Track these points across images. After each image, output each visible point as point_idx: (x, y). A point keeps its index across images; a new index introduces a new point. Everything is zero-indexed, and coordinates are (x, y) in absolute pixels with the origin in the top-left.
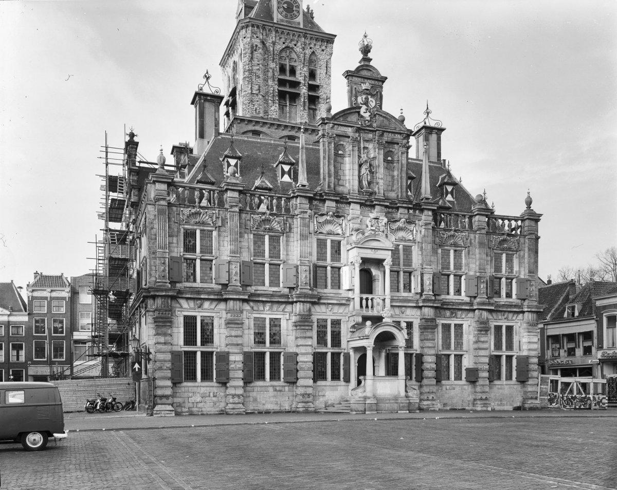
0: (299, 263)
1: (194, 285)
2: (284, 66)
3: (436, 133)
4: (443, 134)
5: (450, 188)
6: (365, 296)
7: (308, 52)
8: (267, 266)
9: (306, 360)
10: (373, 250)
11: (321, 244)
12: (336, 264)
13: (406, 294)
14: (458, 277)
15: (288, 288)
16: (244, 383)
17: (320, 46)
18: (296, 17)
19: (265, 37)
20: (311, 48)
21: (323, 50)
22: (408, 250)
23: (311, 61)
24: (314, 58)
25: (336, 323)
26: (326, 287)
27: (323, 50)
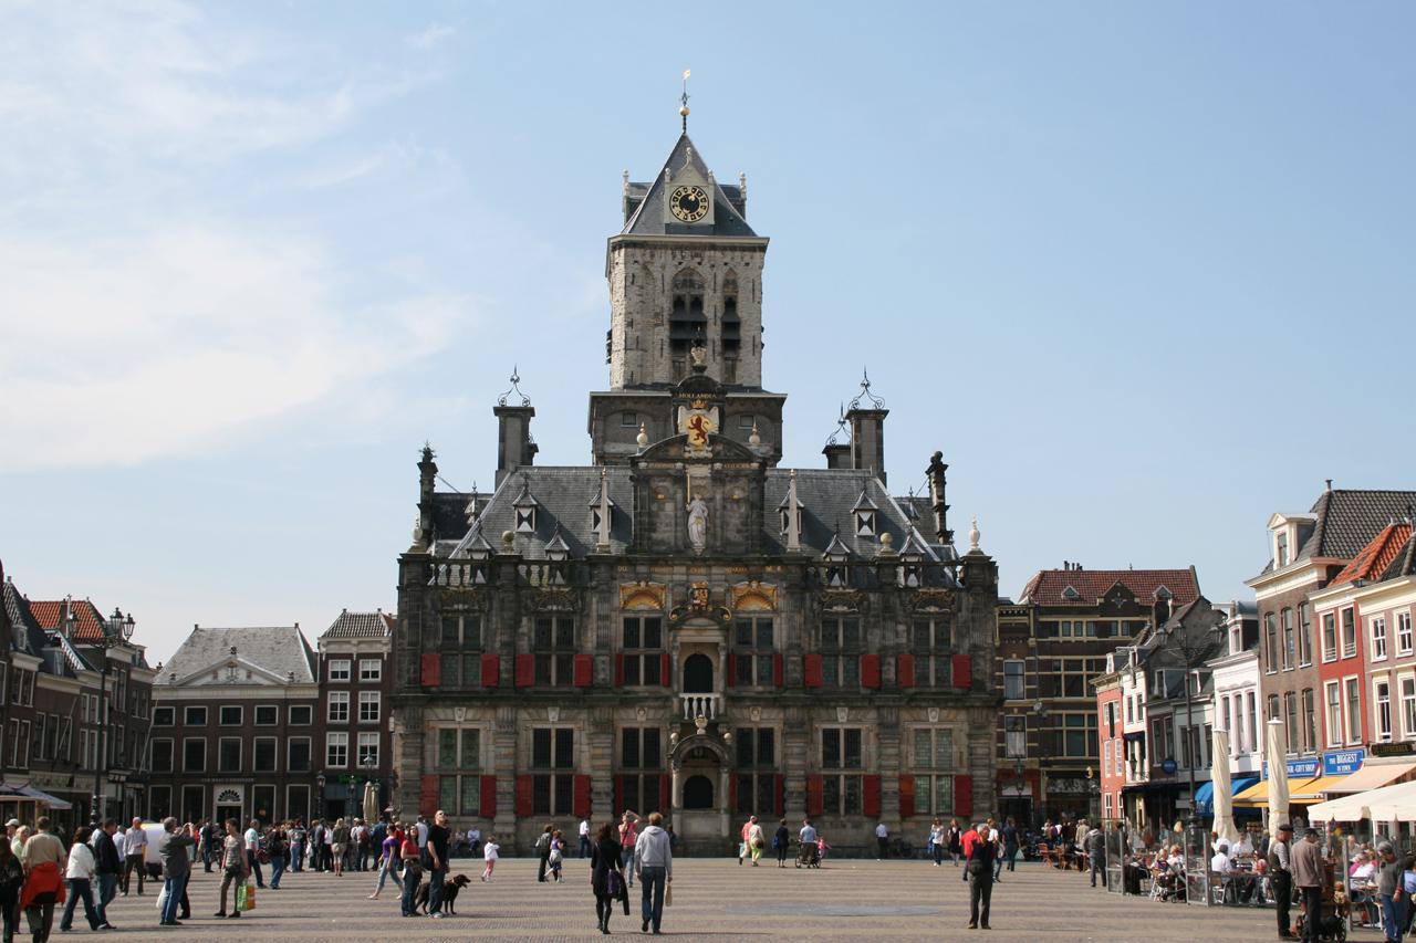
0: (595, 652)
1: (454, 689)
3: (875, 418)
4: (886, 422)
6: (687, 696)
8: (554, 659)
9: (602, 785)
11: (631, 624)
12: (653, 651)
13: (760, 689)
15: (581, 687)
16: (517, 818)
17: (742, 258)
19: (648, 258)
20: (726, 264)
21: (747, 264)
22: (767, 626)
23: (727, 283)
24: (731, 277)
25: (653, 735)
26: (638, 683)
27: (747, 264)
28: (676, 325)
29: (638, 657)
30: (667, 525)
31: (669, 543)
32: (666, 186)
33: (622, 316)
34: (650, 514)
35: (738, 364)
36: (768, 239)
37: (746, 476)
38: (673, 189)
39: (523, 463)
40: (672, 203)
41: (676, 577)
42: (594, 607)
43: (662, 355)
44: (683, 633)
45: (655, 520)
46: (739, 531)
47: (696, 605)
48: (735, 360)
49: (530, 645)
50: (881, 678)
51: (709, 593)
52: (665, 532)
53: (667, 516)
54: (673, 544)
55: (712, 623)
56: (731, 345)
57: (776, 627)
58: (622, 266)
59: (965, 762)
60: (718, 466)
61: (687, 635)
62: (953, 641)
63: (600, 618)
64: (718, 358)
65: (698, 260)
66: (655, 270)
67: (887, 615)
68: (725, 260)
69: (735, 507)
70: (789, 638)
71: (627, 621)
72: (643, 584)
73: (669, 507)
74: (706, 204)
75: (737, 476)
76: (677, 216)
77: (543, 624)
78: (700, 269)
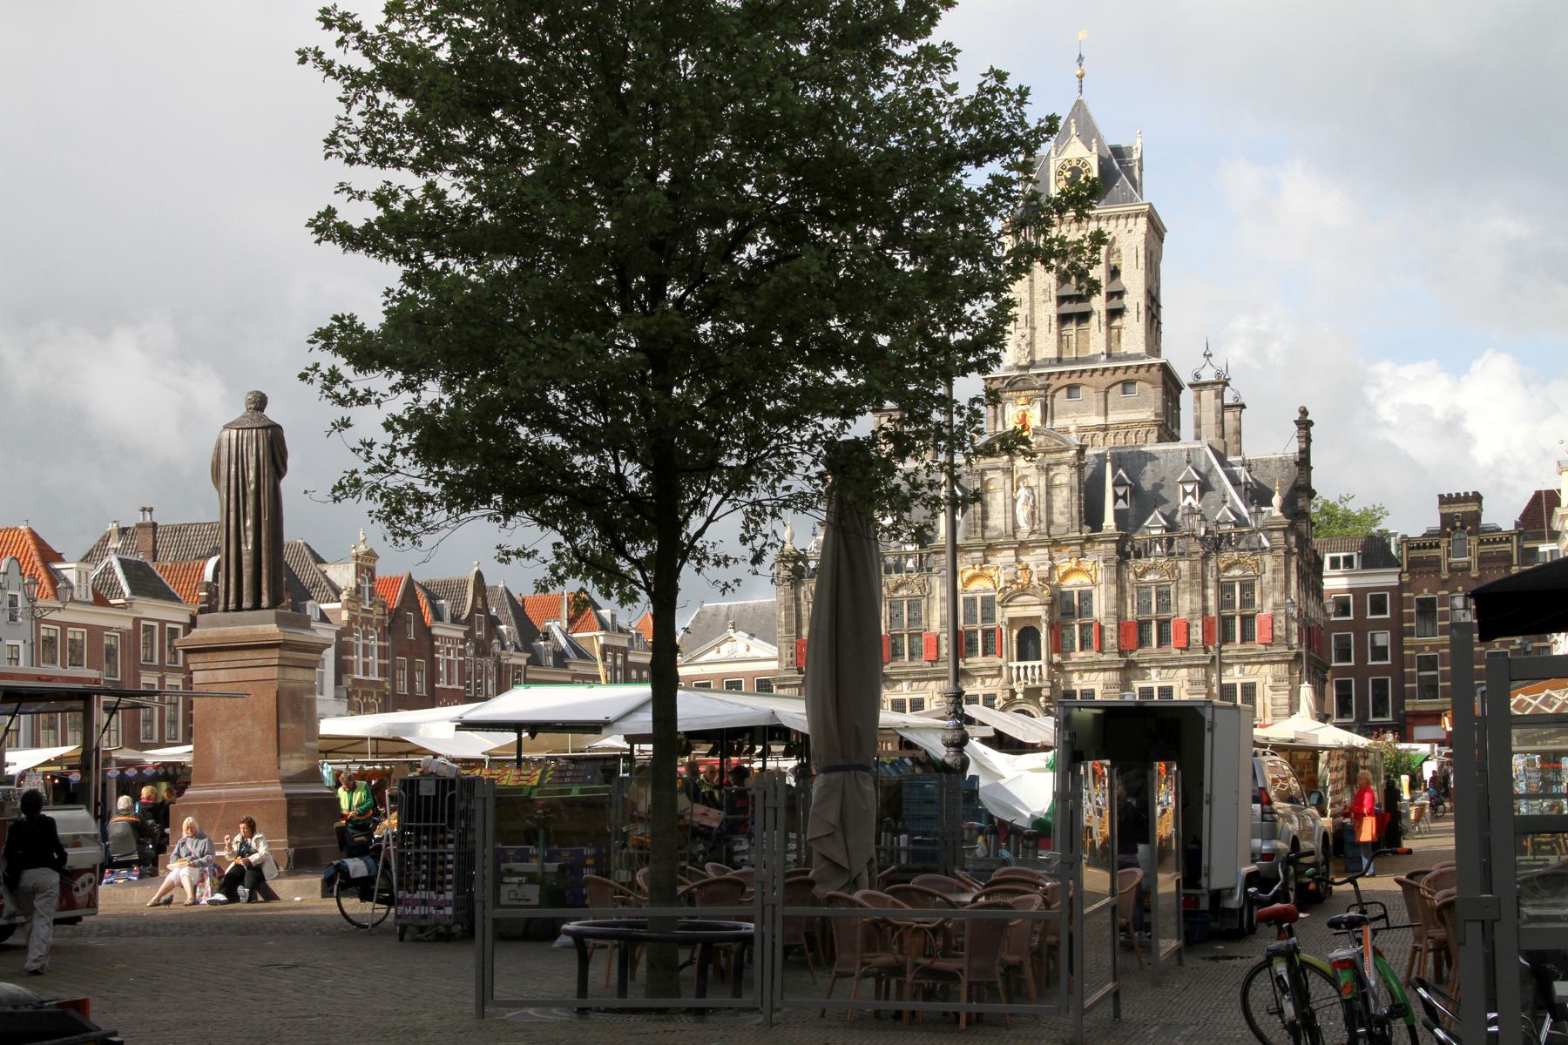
5: (1189, 488)
6: (1015, 664)
12: (989, 626)
13: (1082, 654)
22: (1086, 597)
28: (1062, 300)
35: (1123, 332)
46: (1062, 513)
48: (1119, 328)
56: (1115, 313)
57: (1095, 598)
59: (1269, 713)
61: (1014, 612)
62: (1257, 601)
64: (1104, 328)
73: (1000, 496)
75: (1058, 464)
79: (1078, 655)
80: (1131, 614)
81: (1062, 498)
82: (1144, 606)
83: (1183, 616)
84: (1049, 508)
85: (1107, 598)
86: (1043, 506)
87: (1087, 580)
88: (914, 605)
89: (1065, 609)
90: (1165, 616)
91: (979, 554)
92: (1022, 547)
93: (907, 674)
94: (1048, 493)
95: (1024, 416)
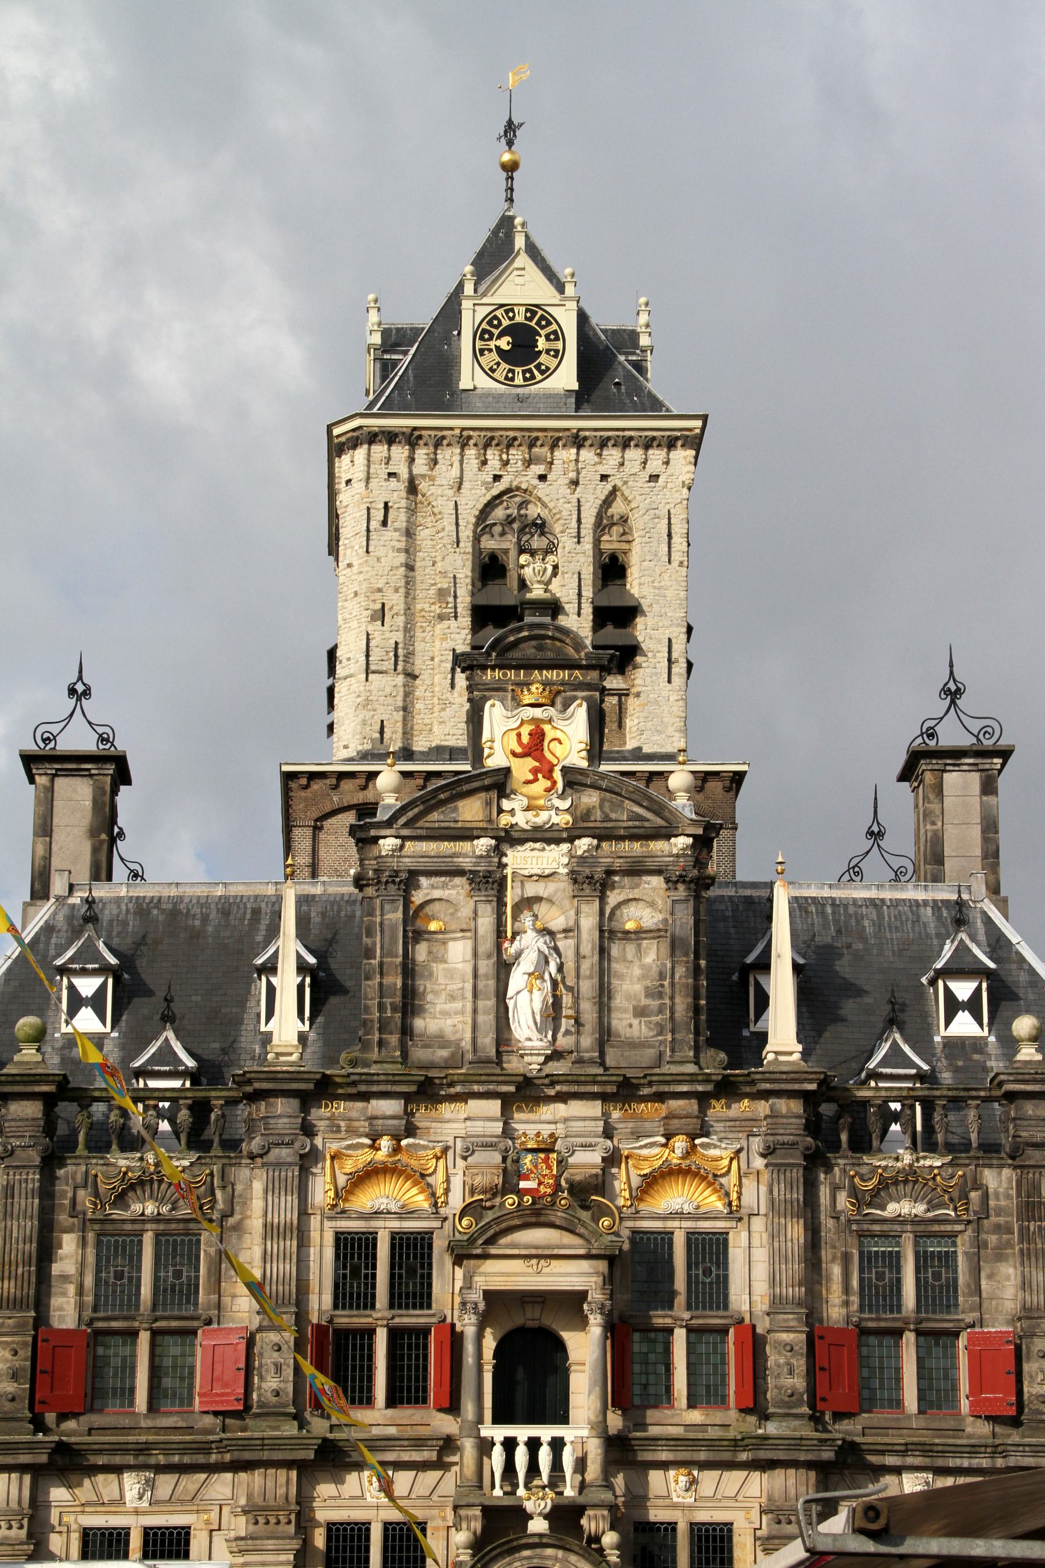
2: (502, 557)
7: (592, 496)
10: (534, 1261)
14: (936, 1339)
18: (546, 372)
19: (420, 467)
20: (604, 478)
29: (371, 1332)
30: (452, 998)
31: (458, 1046)
32: (466, 305)
33: (361, 598)
34: (409, 970)
36: (705, 418)
37: (658, 872)
38: (482, 312)
39: (96, 877)
40: (479, 344)
41: (477, 1127)
42: (257, 1204)
43: (453, 685)
44: (490, 1266)
45: (421, 984)
46: (640, 1012)
47: (527, 1191)
49: (81, 1306)
50: (1020, 1393)
51: (559, 1162)
52: (446, 1014)
53: (451, 974)
54: (466, 1044)
55: (568, 1238)
58: (358, 486)
60: (584, 844)
61: (503, 1274)
63: (270, 1231)
65: (540, 469)
66: (438, 491)
67: (1032, 1226)
68: (603, 470)
69: (630, 949)
70: (773, 1282)
71: (342, 1240)
72: (385, 1143)
74: (559, 345)
76: (490, 372)
77: (114, 1247)
78: (542, 490)
79: (680, 1416)
80: (836, 1310)
81: (638, 970)
82: (879, 1291)
83: (997, 1326)
84: (604, 994)
85: (776, 1257)
86: (588, 987)
87: (714, 1203)
88: (178, 1245)
89: (649, 1282)
90: (941, 1322)
91: (391, 1107)
92: (526, 1092)
93: (144, 1449)
94: (603, 951)
95: (538, 736)
